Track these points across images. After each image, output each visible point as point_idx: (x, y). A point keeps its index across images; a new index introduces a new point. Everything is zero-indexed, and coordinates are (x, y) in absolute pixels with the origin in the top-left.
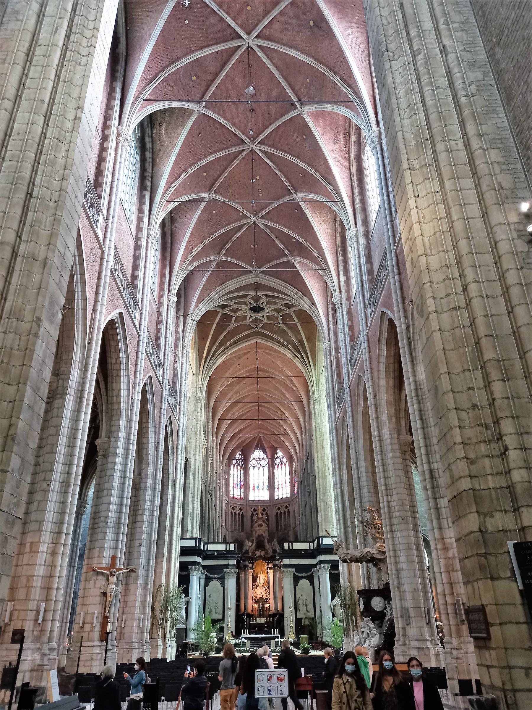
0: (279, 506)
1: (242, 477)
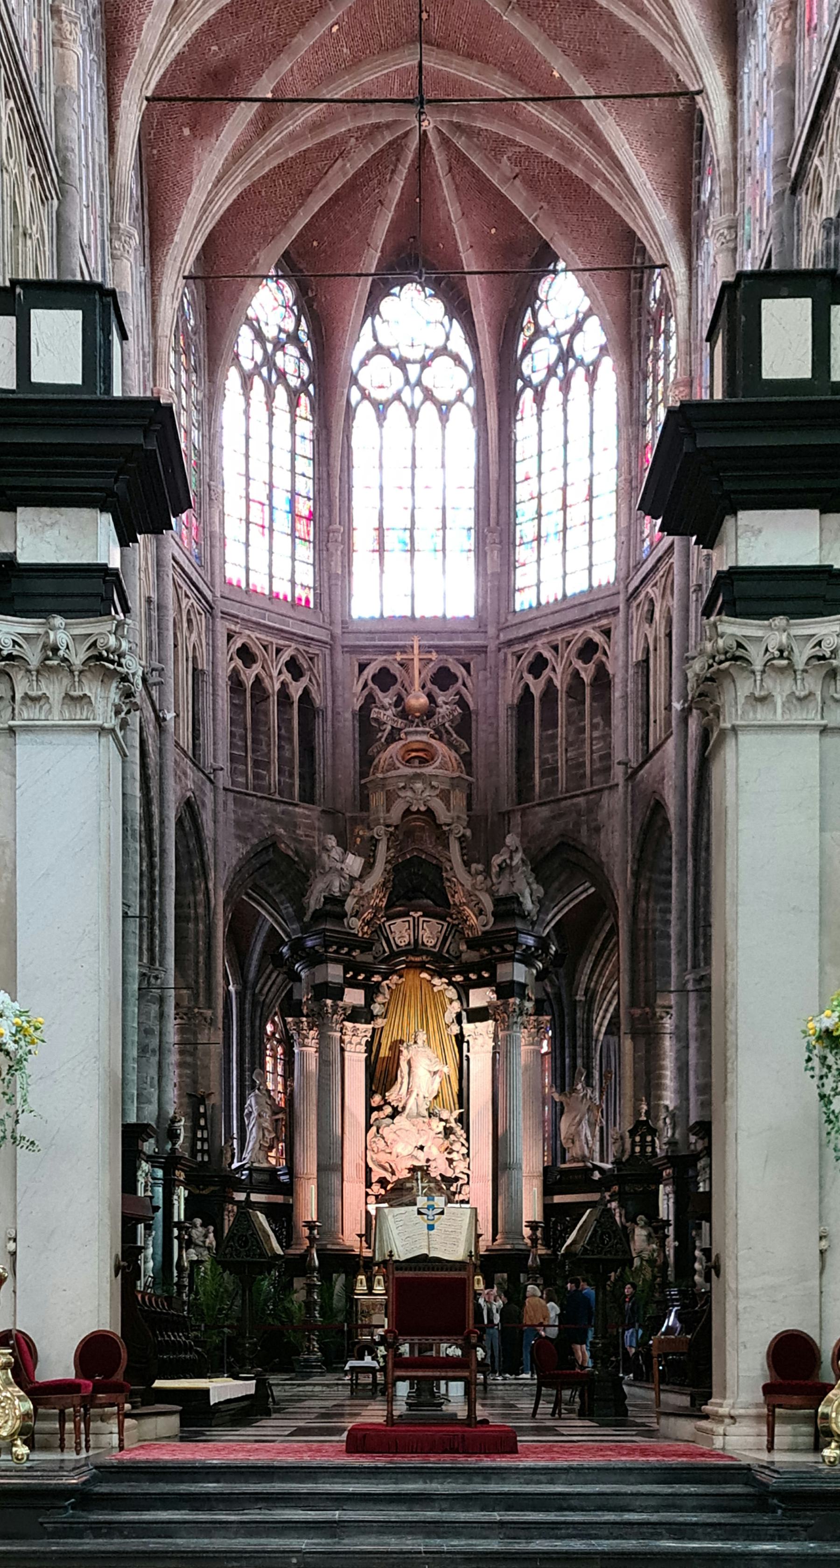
0: (541, 646)
1: (305, 467)
